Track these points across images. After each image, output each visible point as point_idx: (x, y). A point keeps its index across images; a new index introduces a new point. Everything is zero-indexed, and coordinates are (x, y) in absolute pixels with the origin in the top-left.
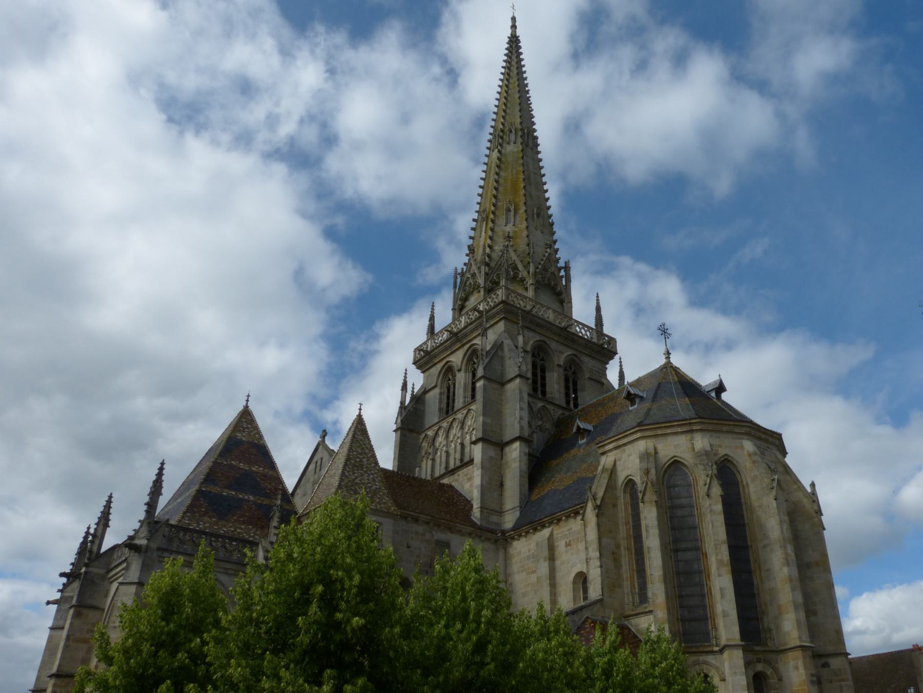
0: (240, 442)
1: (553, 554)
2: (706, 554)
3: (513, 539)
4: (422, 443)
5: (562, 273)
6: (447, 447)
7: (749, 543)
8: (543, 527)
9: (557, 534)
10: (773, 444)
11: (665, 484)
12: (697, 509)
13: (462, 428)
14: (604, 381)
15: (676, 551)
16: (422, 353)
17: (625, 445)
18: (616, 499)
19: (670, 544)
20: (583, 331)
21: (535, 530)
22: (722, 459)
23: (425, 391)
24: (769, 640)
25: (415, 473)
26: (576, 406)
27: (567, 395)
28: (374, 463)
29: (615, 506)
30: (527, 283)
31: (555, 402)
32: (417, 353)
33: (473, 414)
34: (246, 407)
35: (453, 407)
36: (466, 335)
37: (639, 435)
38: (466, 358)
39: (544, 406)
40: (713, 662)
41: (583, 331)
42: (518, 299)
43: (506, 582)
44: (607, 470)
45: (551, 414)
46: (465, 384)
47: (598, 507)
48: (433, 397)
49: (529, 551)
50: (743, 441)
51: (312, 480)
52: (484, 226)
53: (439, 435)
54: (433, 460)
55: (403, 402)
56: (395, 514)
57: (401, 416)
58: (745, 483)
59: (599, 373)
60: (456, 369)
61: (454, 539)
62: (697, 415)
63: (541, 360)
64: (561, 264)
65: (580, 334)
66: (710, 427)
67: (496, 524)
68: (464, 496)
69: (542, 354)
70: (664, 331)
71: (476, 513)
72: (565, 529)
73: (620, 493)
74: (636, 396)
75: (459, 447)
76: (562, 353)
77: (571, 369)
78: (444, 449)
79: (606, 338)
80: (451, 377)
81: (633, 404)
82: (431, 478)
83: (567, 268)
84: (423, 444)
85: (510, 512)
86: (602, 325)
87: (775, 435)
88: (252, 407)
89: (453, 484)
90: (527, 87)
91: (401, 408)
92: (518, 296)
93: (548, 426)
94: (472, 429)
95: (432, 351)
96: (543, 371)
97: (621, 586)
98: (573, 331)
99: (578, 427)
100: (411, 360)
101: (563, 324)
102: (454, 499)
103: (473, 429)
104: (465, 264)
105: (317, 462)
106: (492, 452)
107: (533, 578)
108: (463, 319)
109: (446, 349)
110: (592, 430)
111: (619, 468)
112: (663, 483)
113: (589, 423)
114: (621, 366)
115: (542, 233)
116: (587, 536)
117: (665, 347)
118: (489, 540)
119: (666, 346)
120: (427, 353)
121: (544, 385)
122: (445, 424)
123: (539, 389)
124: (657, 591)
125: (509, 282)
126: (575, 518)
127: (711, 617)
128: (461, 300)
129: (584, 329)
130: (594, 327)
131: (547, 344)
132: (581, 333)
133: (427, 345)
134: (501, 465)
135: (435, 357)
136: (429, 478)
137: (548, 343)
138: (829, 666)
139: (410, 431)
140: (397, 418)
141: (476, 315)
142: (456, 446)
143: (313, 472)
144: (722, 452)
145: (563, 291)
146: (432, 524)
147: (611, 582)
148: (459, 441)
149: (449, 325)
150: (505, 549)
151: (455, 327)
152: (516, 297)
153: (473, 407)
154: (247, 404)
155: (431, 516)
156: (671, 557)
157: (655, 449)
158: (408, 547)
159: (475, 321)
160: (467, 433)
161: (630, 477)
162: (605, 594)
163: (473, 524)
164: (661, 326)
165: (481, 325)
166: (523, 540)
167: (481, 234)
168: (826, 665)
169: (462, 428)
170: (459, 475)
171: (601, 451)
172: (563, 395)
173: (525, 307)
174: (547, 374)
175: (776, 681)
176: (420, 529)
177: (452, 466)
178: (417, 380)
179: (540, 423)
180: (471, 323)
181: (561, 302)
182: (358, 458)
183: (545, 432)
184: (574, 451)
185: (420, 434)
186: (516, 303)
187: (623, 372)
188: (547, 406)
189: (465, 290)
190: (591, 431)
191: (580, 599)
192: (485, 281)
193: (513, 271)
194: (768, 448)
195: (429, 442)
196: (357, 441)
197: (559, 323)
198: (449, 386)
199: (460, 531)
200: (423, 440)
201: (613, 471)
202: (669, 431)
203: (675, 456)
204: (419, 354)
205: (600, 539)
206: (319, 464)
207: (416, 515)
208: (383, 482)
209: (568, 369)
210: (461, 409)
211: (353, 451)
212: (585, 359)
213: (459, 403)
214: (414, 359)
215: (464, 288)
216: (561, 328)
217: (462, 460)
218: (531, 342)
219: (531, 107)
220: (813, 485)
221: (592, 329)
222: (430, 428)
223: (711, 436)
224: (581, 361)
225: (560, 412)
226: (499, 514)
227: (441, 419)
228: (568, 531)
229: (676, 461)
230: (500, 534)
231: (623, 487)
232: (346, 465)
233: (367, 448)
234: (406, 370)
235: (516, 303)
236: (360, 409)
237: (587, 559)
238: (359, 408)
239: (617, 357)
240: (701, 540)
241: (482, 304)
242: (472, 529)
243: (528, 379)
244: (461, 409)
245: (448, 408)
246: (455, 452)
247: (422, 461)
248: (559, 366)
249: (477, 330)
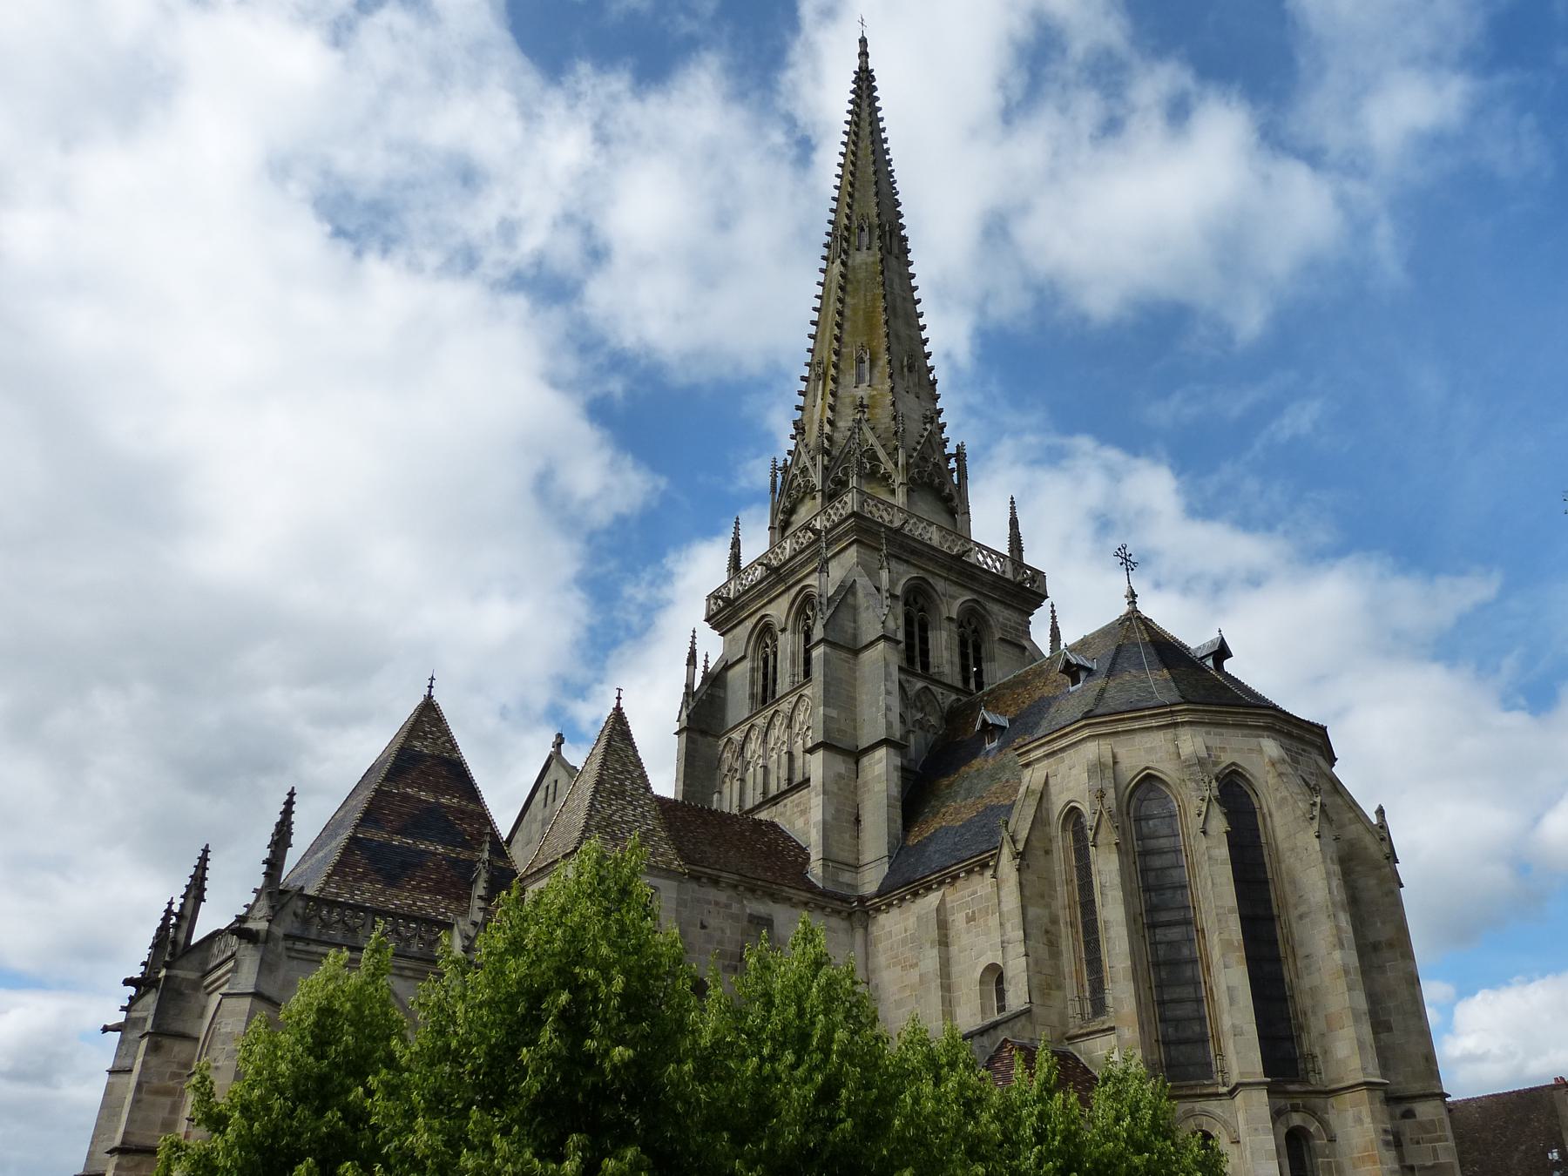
0: (420, 757)
1: (946, 936)
2: (1203, 930)
3: (878, 910)
5: (953, 464)
7: (1275, 911)
8: (929, 889)
9: (952, 902)
10: (1312, 744)
11: (1132, 815)
12: (1187, 856)
13: (789, 726)
14: (1026, 643)
15: (1153, 926)
16: (720, 602)
17: (1062, 750)
18: (1051, 840)
19: (1141, 914)
20: (989, 561)
21: (916, 895)
22: (1227, 771)
23: (727, 667)
24: (1312, 1074)
25: (712, 801)
26: (980, 686)
27: (965, 668)
28: (643, 788)
29: (1048, 852)
30: (894, 481)
31: (945, 681)
32: (712, 602)
33: (808, 703)
34: (430, 697)
35: (774, 692)
36: (793, 572)
37: (1086, 733)
39: (926, 687)
40: (1218, 1111)
41: (989, 561)
42: (879, 510)
43: (868, 984)
44: (1033, 792)
45: (938, 701)
46: (793, 654)
47: (1020, 856)
48: (740, 678)
49: (906, 931)
50: (1261, 739)
51: (540, 817)
52: (820, 387)
53: (751, 738)
54: (742, 780)
55: (689, 686)
56: (680, 873)
57: (687, 708)
58: (1265, 810)
60: (777, 628)
61: (780, 913)
62: (1183, 698)
63: (920, 611)
64: (951, 449)
65: (985, 566)
66: (1207, 719)
67: (849, 885)
68: (795, 841)
69: (921, 601)
70: (1126, 560)
71: (815, 870)
72: (966, 892)
73: (1056, 829)
74: (1081, 667)
75: (785, 758)
76: (955, 598)
77: (970, 624)
78: (761, 762)
79: (1029, 572)
80: (769, 642)
81: (1075, 681)
82: (740, 810)
83: (960, 456)
84: (725, 755)
85: (873, 865)
86: (1021, 550)
87: (1316, 730)
88: (437, 698)
89: (776, 820)
90: (888, 154)
91: (686, 694)
92: (879, 505)
93: (933, 720)
94: (806, 727)
95: (737, 599)
96: (924, 628)
97: (1060, 987)
98: (972, 560)
99: (984, 721)
100: (703, 614)
101: (955, 550)
102: (778, 845)
103: (808, 728)
104: (790, 453)
105: (548, 787)
106: (841, 765)
107: (914, 975)
108: (787, 544)
109: (760, 595)
110: (1008, 726)
111: (1053, 789)
112: (1128, 814)
113: (1003, 714)
114: (1054, 618)
115: (918, 398)
116: (1001, 906)
117: (1127, 585)
118: (839, 912)
119: (1129, 583)
120: (728, 602)
121: (925, 653)
122: (760, 721)
123: (918, 659)
124: (1122, 993)
125: (863, 481)
126: (982, 874)
127: (1213, 1036)
128: (783, 512)
129: (991, 557)
130: (1008, 554)
131: (929, 583)
132: (987, 564)
133: (729, 589)
134: (856, 787)
135: (742, 608)
136: (735, 811)
137: (931, 581)
138: (1414, 1116)
139: (704, 733)
140: (680, 712)
141: (810, 538)
142: (779, 756)
143: (543, 804)
144: (1226, 759)
145: (955, 494)
146: (741, 888)
147: (1045, 982)
149: (765, 555)
150: (866, 929)
151: (775, 558)
152: (876, 506)
153: (807, 691)
154: (430, 692)
155: (740, 875)
156: (1144, 936)
157: (1114, 756)
158: (703, 927)
159: (808, 547)
160: (798, 734)
161: (1071, 804)
162: (1033, 1000)
163: (811, 887)
164: (1119, 549)
165: (818, 553)
166: (895, 912)
167: (815, 401)
168: (1409, 1114)
170: (785, 806)
171: (1023, 761)
172: (957, 669)
173: (891, 522)
174: (930, 634)
175: (1326, 1141)
176: (723, 896)
177: (773, 791)
178: (713, 646)
179: (919, 716)
180: (802, 551)
181: (952, 513)
182: (616, 779)
183: (928, 731)
184: (976, 763)
185: (719, 737)
186: (877, 515)
187: (1058, 628)
188: (930, 687)
189: (790, 496)
190: (1005, 727)
191: (993, 1009)
192: (823, 482)
193: (870, 463)
194: (1303, 750)
195: (734, 751)
196: (615, 750)
197: (949, 547)
198: (767, 656)
199: (790, 899)
201: (1044, 795)
202: (1136, 725)
203: (1147, 768)
204: (715, 604)
205: (1024, 908)
206: (551, 790)
207: (715, 872)
208: (660, 820)
209: (964, 624)
210: (787, 694)
211: (608, 768)
212: (995, 608)
213: (783, 685)
214: (708, 613)
215: (788, 491)
217: (790, 780)
218: (903, 581)
219: (895, 188)
220: (1380, 812)
221: (1004, 556)
222: (735, 727)
223: (1208, 733)
224: (985, 609)
225: (954, 697)
226: (853, 869)
227: (754, 711)
228: (969, 896)
229: (1149, 775)
230: (856, 904)
231: (1061, 821)
232: (596, 791)
233: (631, 762)
234: (694, 632)
235: (877, 515)
236: (619, 698)
237: (1002, 942)
238: (617, 695)
239: (1046, 603)
240: (1194, 908)
241: (818, 519)
242: (809, 895)
243: (898, 642)
244: (787, 694)
245: (766, 695)
246: (779, 768)
247: (724, 782)
248: (950, 619)
249: (811, 562)
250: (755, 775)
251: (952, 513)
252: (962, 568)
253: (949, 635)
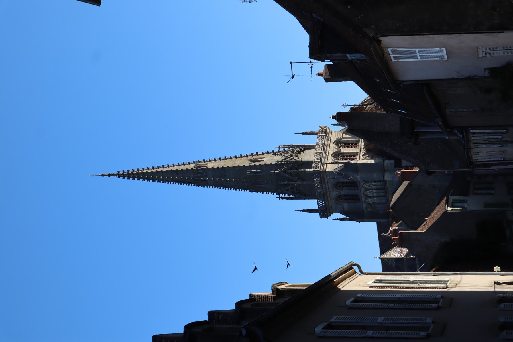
4: (368, 211)
6: (375, 197)
38: (336, 190)
52: (259, 186)
54: (378, 204)
59: (337, 134)
75: (377, 191)
86: (312, 132)
95: (326, 209)
109: (328, 200)
135: (329, 206)
140: (357, 222)
142: (376, 193)
148: (375, 191)
169: (370, 189)
170: (389, 190)
200: (367, 210)
246: (378, 193)
250: (378, 200)
253: (345, 150)
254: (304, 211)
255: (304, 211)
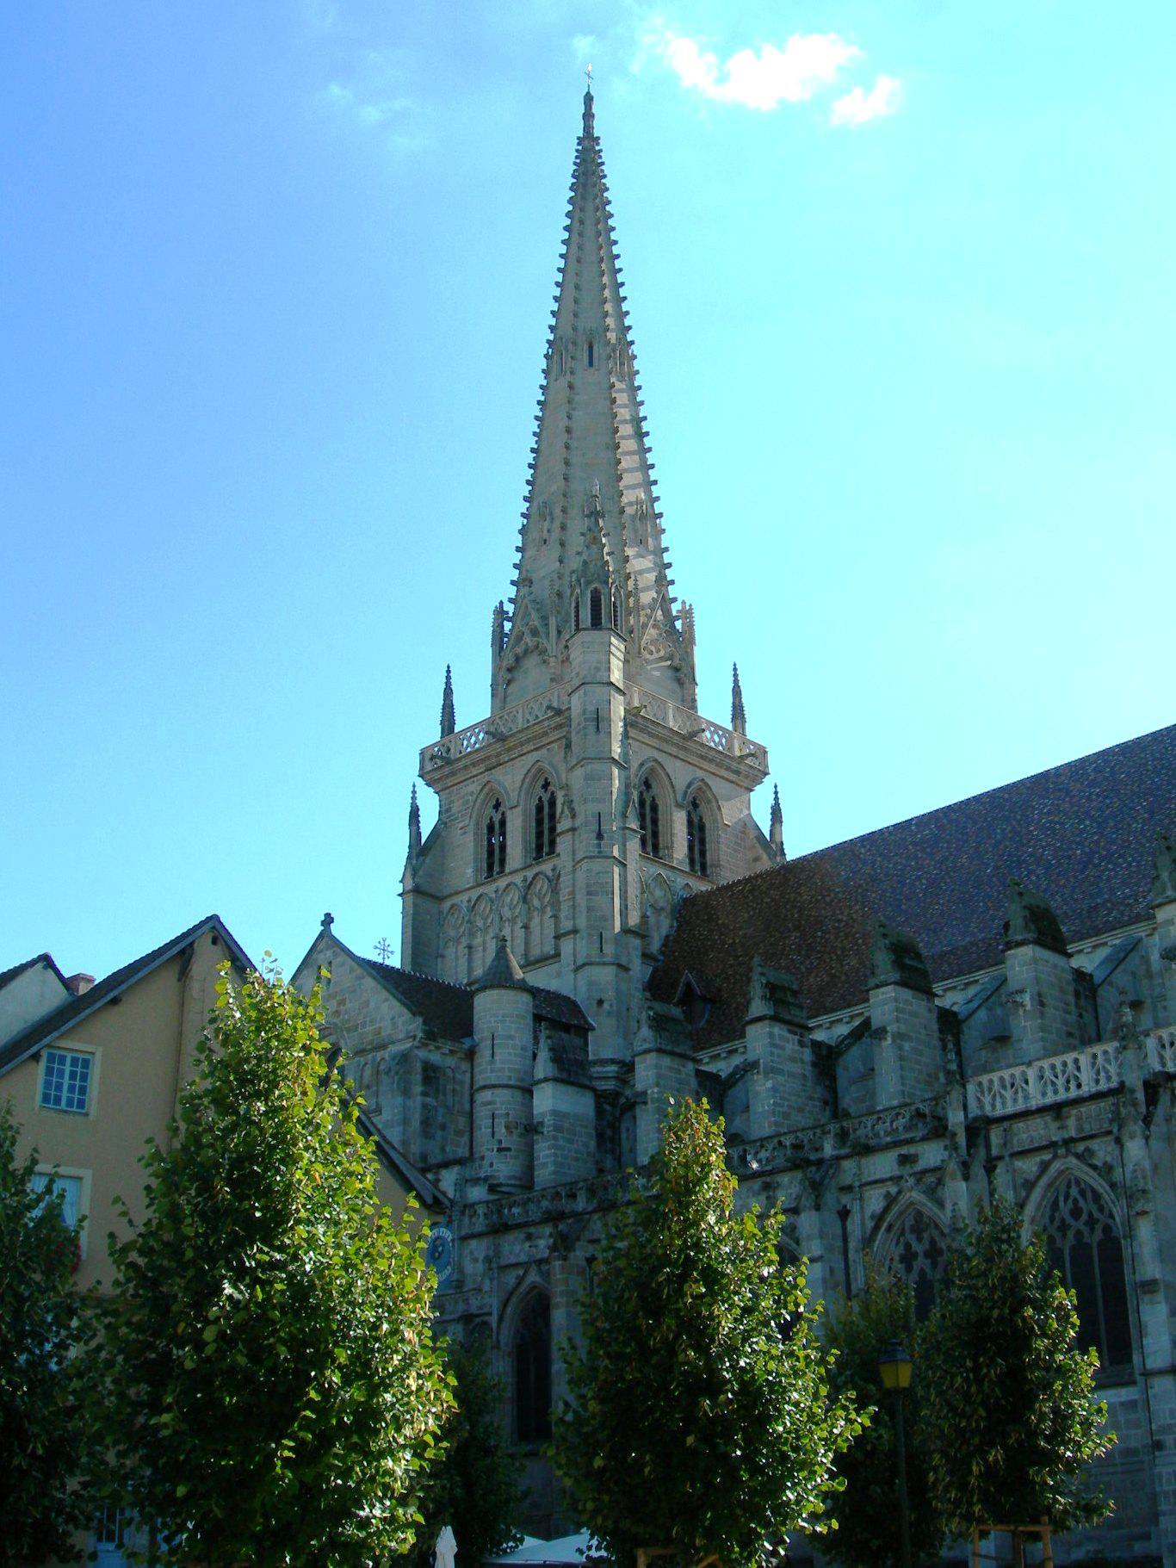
35: (502, 862)
41: (717, 739)
64: (675, 608)
65: (712, 744)
83: (687, 614)
86: (744, 721)
129: (717, 733)
153: (546, 867)
214: (422, 768)
216: (684, 738)
239: (768, 781)
251: (680, 682)
252: (688, 740)
254: (448, 692)
255: (448, 692)
